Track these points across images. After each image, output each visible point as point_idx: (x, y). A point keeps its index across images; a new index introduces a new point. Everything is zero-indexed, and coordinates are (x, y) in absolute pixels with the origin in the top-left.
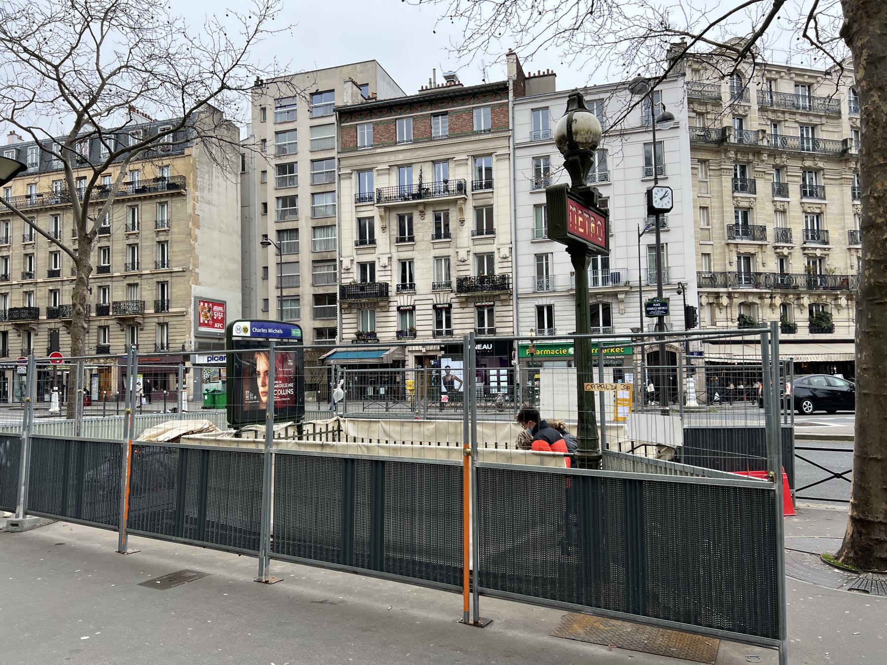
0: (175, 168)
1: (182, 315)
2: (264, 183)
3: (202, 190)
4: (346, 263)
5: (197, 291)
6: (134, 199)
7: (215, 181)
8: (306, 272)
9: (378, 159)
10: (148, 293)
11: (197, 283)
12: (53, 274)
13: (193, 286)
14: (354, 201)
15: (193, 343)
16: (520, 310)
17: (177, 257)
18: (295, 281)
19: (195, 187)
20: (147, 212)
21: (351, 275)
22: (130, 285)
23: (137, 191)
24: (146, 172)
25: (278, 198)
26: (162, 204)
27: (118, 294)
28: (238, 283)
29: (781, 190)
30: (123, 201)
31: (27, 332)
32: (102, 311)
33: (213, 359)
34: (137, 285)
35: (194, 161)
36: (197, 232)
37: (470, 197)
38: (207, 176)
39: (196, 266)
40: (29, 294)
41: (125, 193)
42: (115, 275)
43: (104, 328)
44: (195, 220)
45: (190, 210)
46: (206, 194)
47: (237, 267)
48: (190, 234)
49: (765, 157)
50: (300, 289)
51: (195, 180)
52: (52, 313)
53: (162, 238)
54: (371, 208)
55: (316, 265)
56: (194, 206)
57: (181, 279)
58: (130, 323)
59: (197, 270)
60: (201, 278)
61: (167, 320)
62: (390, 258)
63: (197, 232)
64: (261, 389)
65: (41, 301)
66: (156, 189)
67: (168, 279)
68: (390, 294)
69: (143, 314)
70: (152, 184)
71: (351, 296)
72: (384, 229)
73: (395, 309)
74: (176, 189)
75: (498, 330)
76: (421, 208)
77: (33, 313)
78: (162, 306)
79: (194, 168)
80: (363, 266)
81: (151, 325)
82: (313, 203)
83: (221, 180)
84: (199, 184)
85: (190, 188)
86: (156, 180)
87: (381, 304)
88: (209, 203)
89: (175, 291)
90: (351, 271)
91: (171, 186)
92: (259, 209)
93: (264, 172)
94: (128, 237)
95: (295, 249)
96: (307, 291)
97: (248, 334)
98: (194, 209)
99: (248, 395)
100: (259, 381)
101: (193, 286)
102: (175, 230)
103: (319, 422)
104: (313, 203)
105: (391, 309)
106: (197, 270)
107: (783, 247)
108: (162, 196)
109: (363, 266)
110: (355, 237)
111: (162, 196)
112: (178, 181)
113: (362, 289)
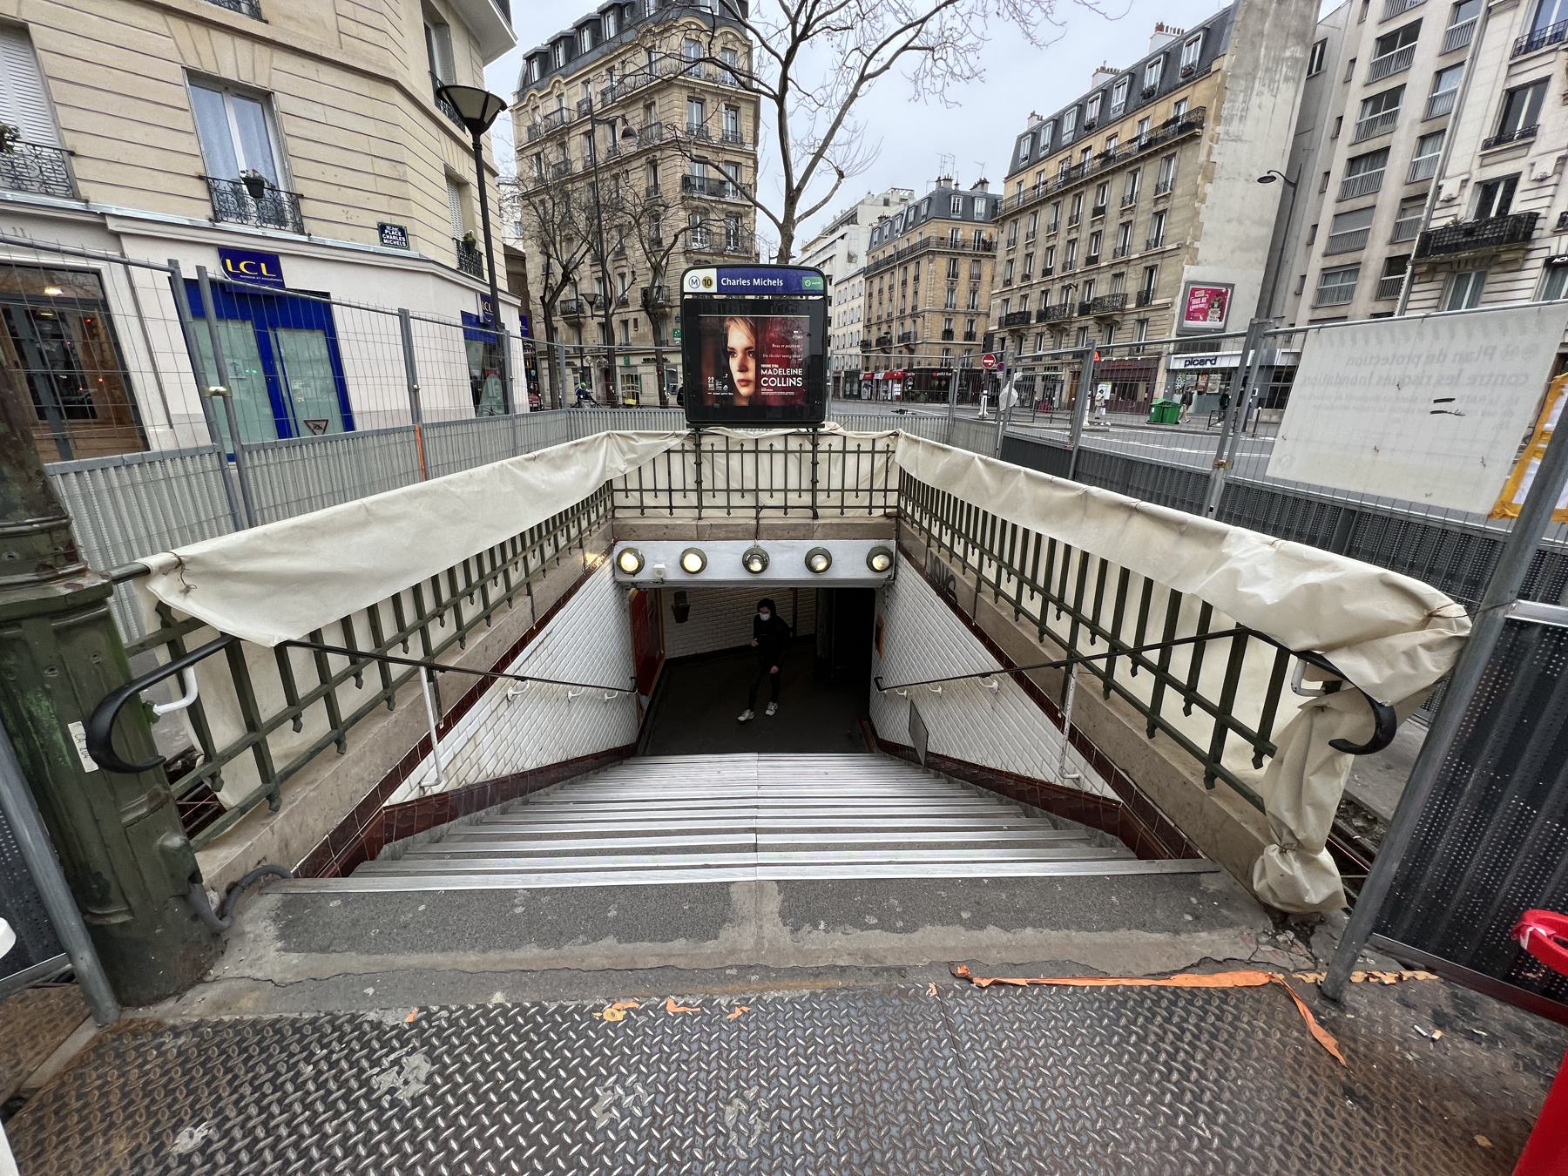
0: (1198, 94)
1: (1166, 307)
2: (1347, 81)
3: (1230, 120)
4: (1450, 187)
5: (1191, 273)
6: (1137, 161)
7: (1255, 100)
8: (1383, 225)
10: (1132, 285)
11: (1194, 262)
12: (1047, 272)
14: (1508, 53)
17: (1173, 229)
18: (1359, 240)
20: (1149, 175)
22: (1116, 276)
23: (1142, 148)
24: (1161, 112)
25: (1365, 101)
26: (1169, 159)
27: (1102, 289)
28: (1262, 255)
30: (1125, 166)
31: (1019, 337)
32: (1084, 309)
33: (1191, 363)
34: (1122, 274)
35: (1225, 76)
36: (1209, 188)
38: (1241, 98)
39: (1196, 238)
40: (1025, 297)
41: (1128, 155)
43: (1083, 329)
44: (1208, 172)
45: (1202, 158)
46: (1235, 128)
47: (1267, 232)
48: (1195, 194)
50: (1365, 253)
51: (1219, 108)
52: (1042, 316)
53: (1160, 207)
54: (1551, 57)
55: (1406, 206)
57: (1173, 260)
58: (1108, 324)
59: (1197, 245)
60: (1200, 256)
61: (1148, 315)
63: (1209, 188)
64: (737, 376)
65: (1033, 306)
66: (1164, 138)
67: (1158, 262)
68: (1536, 234)
69: (1123, 310)
70: (1161, 133)
71: (1438, 250)
73: (1540, 262)
74: (1187, 131)
77: (1024, 317)
78: (1144, 299)
79: (1222, 89)
80: (1488, 189)
81: (1130, 322)
82: (1436, 87)
83: (1267, 99)
84: (1224, 113)
85: (1209, 125)
86: (1167, 124)
87: (1504, 257)
88: (1238, 139)
89: (1163, 277)
91: (1182, 129)
92: (1328, 126)
93: (1353, 61)
94: (1122, 214)
95: (1374, 185)
96: (1376, 253)
97: (714, 289)
98: (1210, 153)
99: (711, 383)
100: (734, 364)
102: (1178, 191)
103: (849, 434)
104: (1436, 87)
105: (1529, 264)
106: (1197, 245)
108: (1170, 146)
109: (1488, 189)
110: (1488, 130)
111: (1170, 146)
112: (1193, 118)
113: (1469, 231)
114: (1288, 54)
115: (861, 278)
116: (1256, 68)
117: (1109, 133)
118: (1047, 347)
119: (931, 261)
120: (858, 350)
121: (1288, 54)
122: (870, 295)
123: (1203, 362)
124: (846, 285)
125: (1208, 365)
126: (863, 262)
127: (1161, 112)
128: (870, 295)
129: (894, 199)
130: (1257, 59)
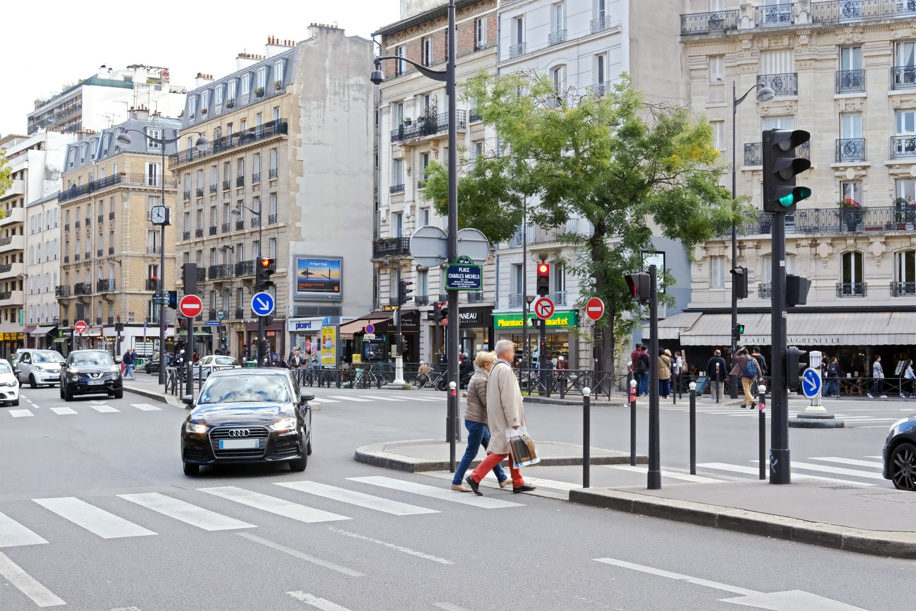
5: (297, 248)
9: (407, 87)
11: (298, 238)
13: (292, 243)
15: (291, 308)
16: (500, 270)
19: (298, 130)
21: (386, 228)
29: (850, 81)
37: (468, 130)
42: (246, 231)
49: (804, 39)
56: (295, 150)
59: (298, 224)
60: (304, 234)
62: (413, 207)
63: (299, 180)
70: (267, 129)
72: (409, 170)
75: (485, 295)
76: (432, 144)
79: (295, 109)
84: (302, 125)
90: (387, 223)
98: (295, 154)
101: (292, 243)
106: (298, 224)
107: (846, 168)
114: (351, 82)
115: (55, 204)
116: (324, 91)
117: (242, 115)
118: (219, 302)
119: (124, 199)
120: (52, 298)
121: (351, 82)
122: (67, 228)
123: (305, 325)
124: (39, 209)
125: (307, 329)
126: (58, 186)
127: (267, 113)
128: (67, 228)
129: (140, 77)
130: (324, 86)
